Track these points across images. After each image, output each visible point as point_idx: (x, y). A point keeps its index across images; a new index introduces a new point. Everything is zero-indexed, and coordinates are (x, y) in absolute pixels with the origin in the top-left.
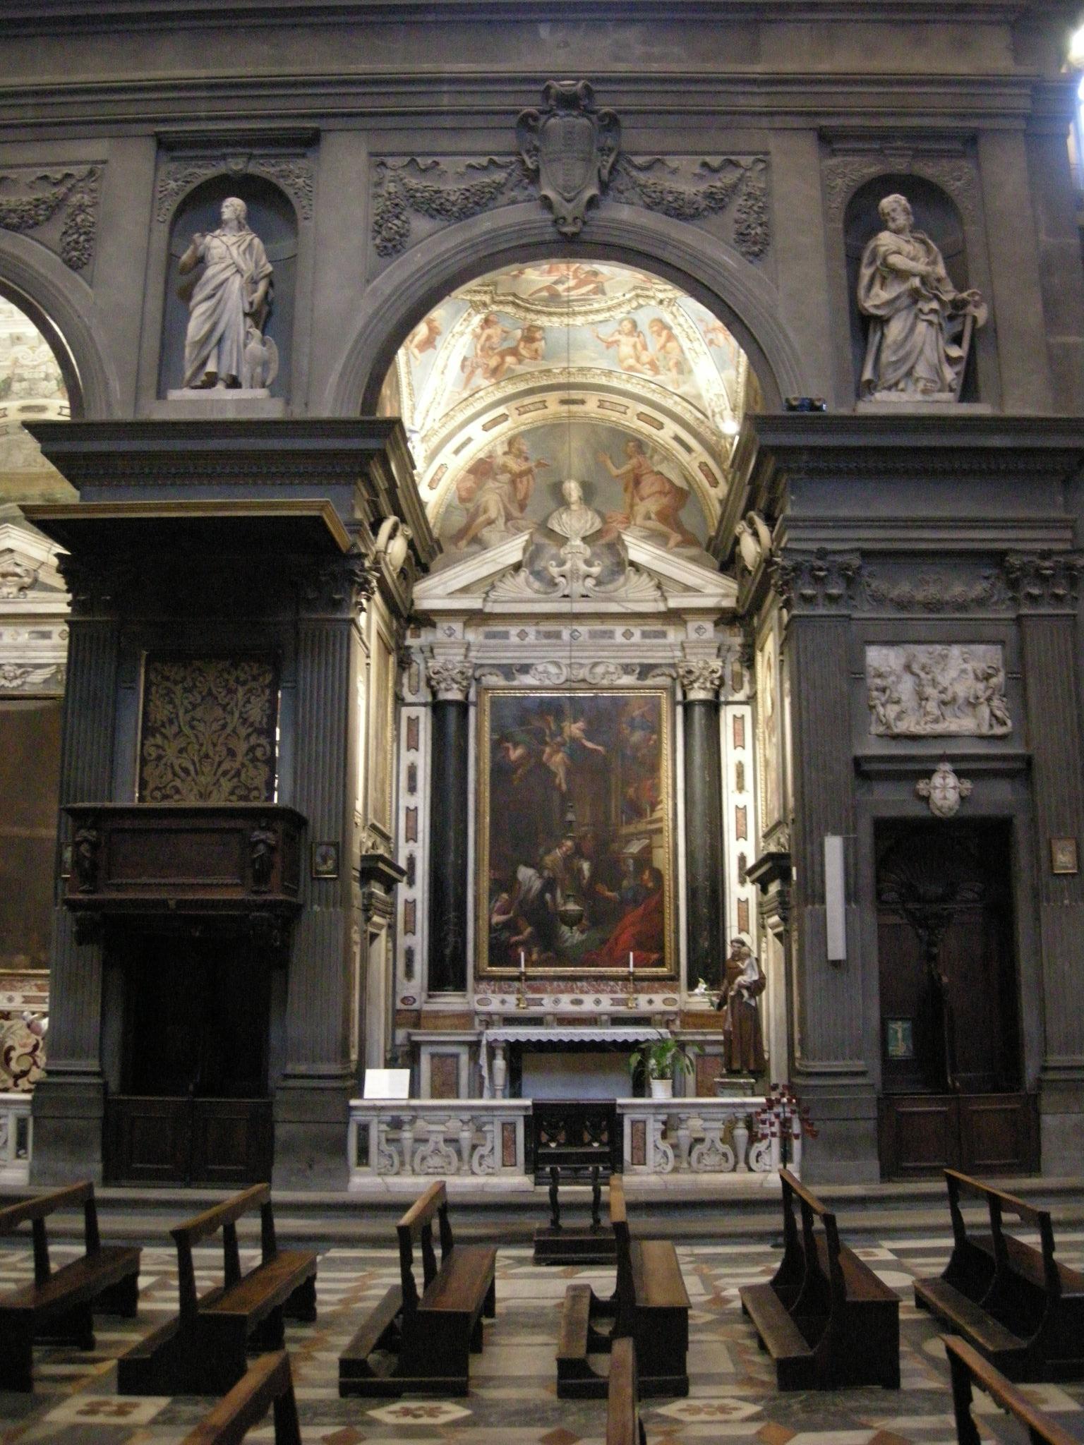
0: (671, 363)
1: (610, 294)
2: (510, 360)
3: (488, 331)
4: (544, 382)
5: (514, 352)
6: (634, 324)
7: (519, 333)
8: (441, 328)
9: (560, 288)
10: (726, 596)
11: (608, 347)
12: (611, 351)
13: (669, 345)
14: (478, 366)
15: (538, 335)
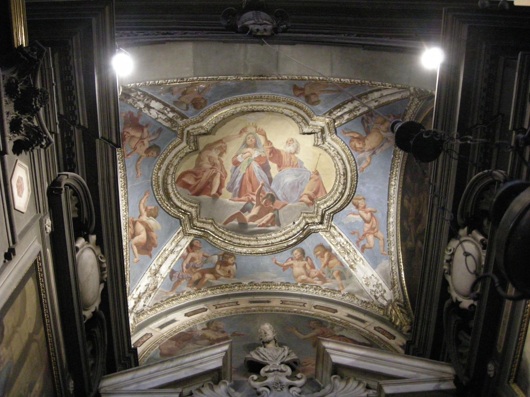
0: (335, 274)
1: (283, 224)
2: (208, 276)
3: (192, 254)
4: (236, 290)
5: (212, 271)
6: (303, 252)
7: (216, 258)
8: (157, 241)
9: (247, 216)
10: (442, 380)
11: (284, 270)
13: (331, 262)
14: (183, 279)
15: (230, 261)
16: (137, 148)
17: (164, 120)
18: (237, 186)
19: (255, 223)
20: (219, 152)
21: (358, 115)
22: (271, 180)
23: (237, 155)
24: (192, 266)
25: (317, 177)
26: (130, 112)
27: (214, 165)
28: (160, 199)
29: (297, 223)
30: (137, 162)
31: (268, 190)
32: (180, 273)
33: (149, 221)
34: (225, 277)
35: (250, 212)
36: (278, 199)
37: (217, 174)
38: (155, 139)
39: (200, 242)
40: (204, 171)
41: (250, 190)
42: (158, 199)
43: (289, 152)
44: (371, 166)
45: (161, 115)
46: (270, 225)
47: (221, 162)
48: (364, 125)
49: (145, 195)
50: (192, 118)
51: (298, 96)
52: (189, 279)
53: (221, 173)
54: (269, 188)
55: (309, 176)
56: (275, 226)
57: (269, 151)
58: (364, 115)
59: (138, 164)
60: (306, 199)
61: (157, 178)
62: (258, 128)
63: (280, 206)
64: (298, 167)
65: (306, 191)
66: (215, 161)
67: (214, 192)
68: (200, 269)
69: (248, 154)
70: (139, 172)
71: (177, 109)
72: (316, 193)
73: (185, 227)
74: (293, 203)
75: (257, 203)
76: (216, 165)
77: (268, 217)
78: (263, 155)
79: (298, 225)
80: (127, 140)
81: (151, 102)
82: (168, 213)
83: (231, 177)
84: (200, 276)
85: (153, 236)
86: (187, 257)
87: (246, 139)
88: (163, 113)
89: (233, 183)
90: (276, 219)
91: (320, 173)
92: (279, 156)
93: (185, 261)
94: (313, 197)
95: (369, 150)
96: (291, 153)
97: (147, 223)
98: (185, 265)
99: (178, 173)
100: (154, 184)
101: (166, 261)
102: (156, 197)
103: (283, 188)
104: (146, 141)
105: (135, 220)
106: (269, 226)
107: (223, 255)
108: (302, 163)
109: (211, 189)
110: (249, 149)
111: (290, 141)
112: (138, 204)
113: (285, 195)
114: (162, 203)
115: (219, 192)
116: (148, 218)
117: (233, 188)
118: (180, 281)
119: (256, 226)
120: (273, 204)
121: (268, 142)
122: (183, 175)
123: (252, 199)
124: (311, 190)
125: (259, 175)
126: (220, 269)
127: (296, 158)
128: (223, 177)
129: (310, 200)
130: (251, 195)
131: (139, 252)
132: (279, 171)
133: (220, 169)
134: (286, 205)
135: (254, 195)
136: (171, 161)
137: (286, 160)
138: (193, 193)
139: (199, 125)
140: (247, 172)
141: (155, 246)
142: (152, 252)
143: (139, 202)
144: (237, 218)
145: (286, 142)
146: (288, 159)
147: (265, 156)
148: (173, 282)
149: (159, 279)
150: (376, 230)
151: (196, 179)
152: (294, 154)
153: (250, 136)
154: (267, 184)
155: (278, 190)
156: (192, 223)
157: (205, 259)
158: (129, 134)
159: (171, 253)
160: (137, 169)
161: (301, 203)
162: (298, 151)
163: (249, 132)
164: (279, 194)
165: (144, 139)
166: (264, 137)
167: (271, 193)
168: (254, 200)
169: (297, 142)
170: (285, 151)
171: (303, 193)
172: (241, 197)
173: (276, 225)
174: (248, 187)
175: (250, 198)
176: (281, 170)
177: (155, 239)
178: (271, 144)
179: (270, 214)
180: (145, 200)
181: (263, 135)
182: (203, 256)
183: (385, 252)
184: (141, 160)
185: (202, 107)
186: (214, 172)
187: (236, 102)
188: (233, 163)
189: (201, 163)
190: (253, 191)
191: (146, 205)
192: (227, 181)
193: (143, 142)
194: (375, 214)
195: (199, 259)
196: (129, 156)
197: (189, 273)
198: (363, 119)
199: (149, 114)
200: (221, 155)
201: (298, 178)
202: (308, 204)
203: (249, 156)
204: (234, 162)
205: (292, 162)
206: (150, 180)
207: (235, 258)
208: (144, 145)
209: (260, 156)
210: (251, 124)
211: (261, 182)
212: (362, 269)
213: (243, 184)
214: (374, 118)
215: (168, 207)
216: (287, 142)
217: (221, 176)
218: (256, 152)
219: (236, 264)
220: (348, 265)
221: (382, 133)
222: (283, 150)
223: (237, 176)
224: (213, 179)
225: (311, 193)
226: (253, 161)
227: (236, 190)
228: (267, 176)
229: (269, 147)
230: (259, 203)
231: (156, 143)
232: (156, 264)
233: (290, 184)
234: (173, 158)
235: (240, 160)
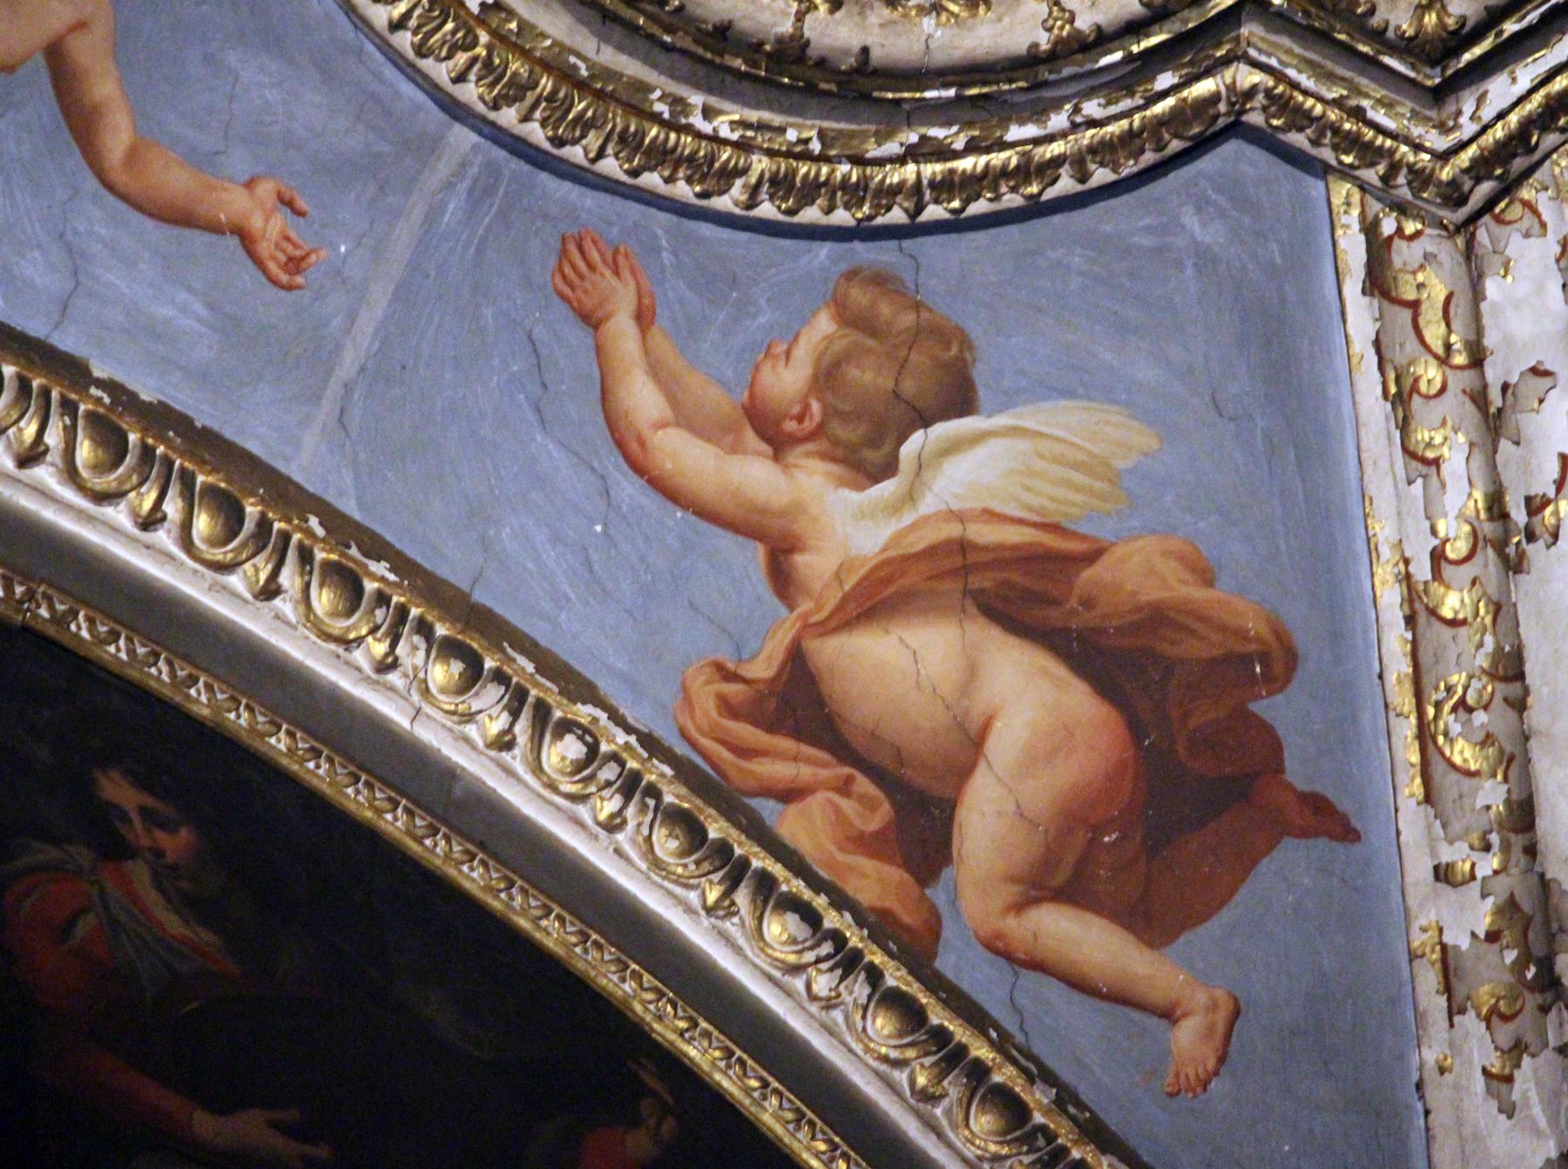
28: (780, 185)
33: (929, 504)
42: (767, 210)
49: (592, 320)
61: (498, 36)
70: (234, 203)
73: (1370, 154)
82: (1036, 210)
85: (1152, 593)
97: (931, 552)
100: (536, 133)
101: (1536, 716)
102: (723, 203)
112: (629, 488)
114: (854, 193)
116: (887, 488)
142: (1298, 771)
143: (612, 462)
156: (1378, 36)
159: (1514, 565)
160: (180, 217)
177: (1198, 594)
180: (656, 371)
184: (104, 87)
191: (718, 399)
206: (463, 137)
215: (966, 164)
232: (1458, 854)
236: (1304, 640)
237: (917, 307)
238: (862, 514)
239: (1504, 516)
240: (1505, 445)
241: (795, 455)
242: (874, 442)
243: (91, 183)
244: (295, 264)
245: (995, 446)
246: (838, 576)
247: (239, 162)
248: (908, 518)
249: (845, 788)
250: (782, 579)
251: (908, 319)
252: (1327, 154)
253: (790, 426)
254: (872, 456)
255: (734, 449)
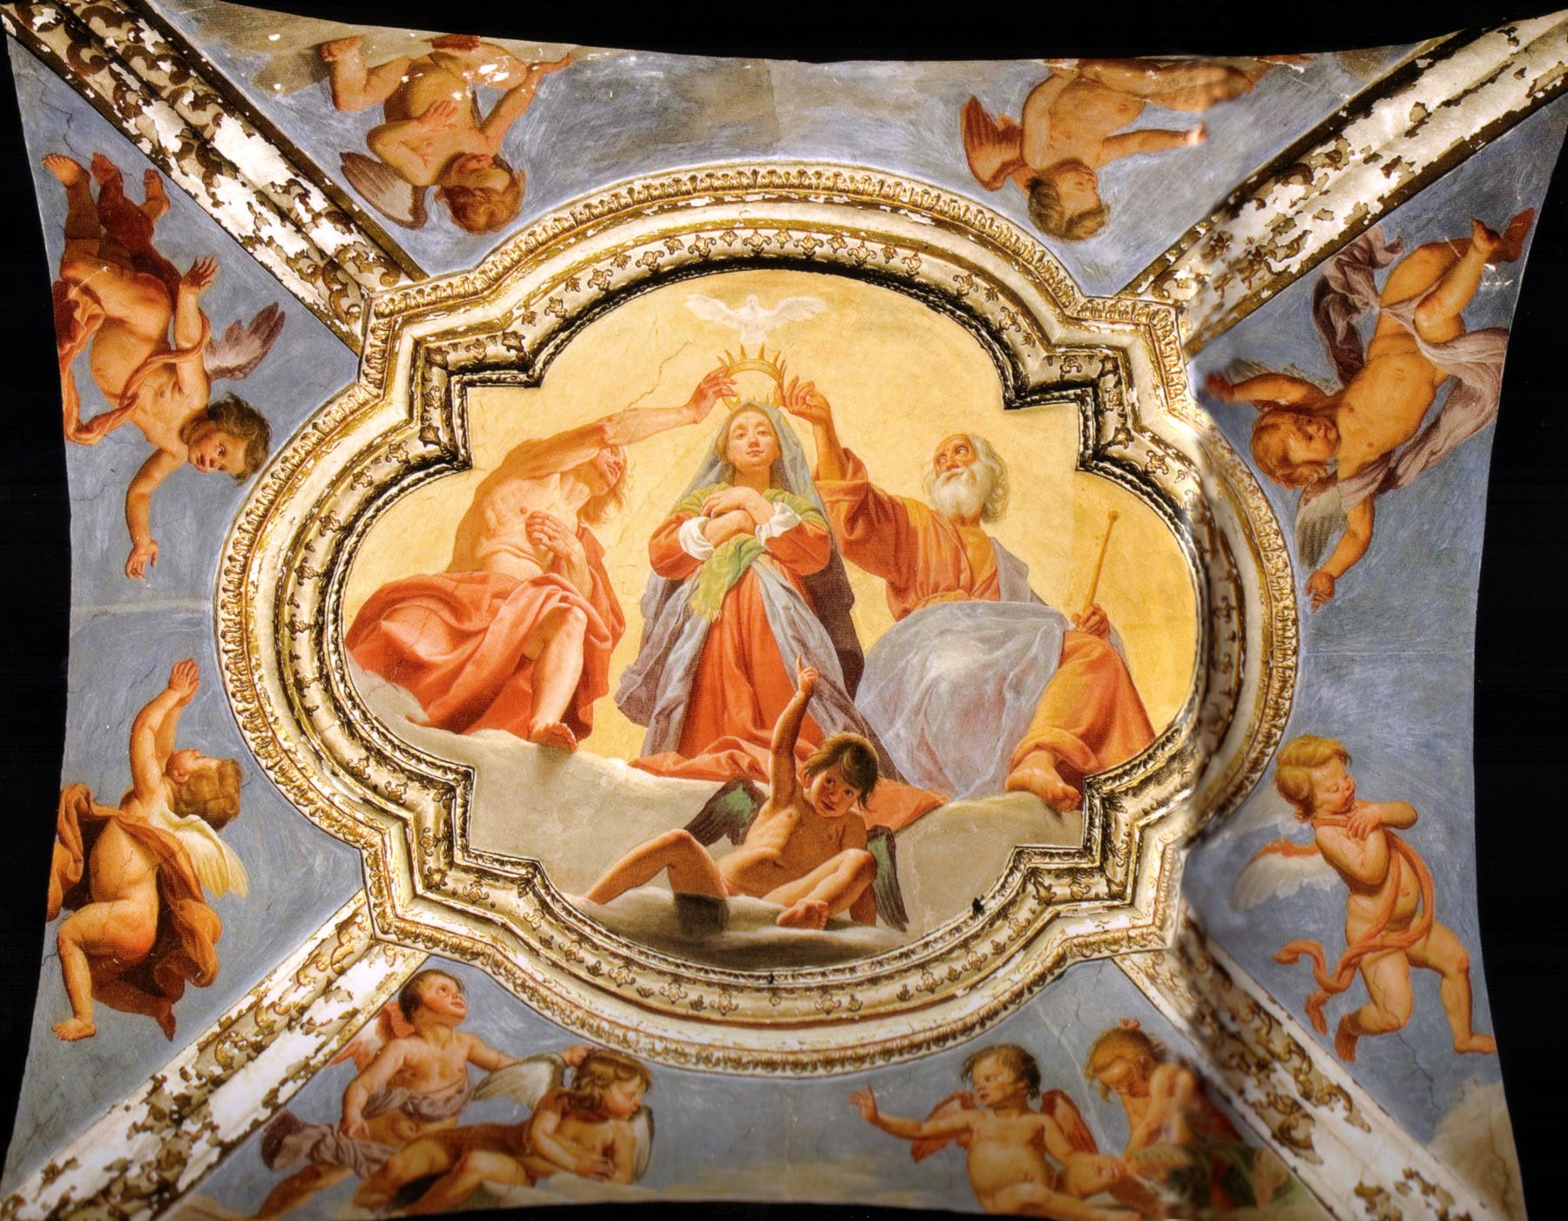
2: (486, 1166)
3: (407, 1048)
7: (540, 1078)
8: (215, 957)
9: (725, 859)
12: (936, 1163)
14: (339, 1163)
15: (620, 1095)
16: (139, 401)
17: (288, 260)
18: (674, 689)
19: (767, 903)
20: (584, 493)
21: (1294, 269)
22: (853, 664)
23: (679, 521)
24: (403, 1108)
25: (1097, 648)
26: (101, 165)
27: (557, 562)
29: (992, 906)
30: (135, 482)
31: (841, 719)
32: (324, 1136)
33: (180, 835)
34: (581, 1173)
35: (738, 839)
36: (891, 773)
37: (571, 617)
38: (240, 368)
39: (460, 987)
40: (502, 595)
41: (742, 715)
43: (948, 511)
44: (1372, 560)
45: (274, 228)
46: (845, 915)
47: (594, 554)
48: (1329, 329)
49: (171, 685)
50: (440, 278)
51: (990, 184)
52: (376, 1168)
53: (593, 611)
54: (846, 709)
55: (1058, 642)
56: (873, 923)
57: (844, 508)
58: (1328, 268)
59: (142, 496)
60: (1041, 772)
62: (787, 381)
63: (903, 815)
64: (998, 591)
65: (1044, 729)
66: (560, 545)
67: (550, 713)
68: (446, 1124)
69: (734, 518)
70: (144, 539)
71: (359, 204)
72: (1095, 739)
74: (972, 797)
75: (777, 790)
76: (564, 564)
77: (836, 869)
78: (816, 524)
79: (1003, 913)
80: (85, 335)
81: (217, 120)
83: (646, 639)
84: (441, 1158)
85: (198, 926)
86: (377, 1057)
87: (727, 438)
88: (284, 215)
89: (652, 676)
90: (878, 884)
91: (1115, 622)
92: (898, 534)
93: (366, 1079)
94: (1078, 760)
95: (1361, 471)
96: (962, 520)
97: (164, 845)
98: (360, 1098)
99: (358, 591)
103: (917, 711)
104: (189, 369)
105: (98, 810)
106: (841, 925)
107: (583, 1067)
108: (1020, 570)
109: (534, 699)
110: (741, 493)
111: (957, 450)
112: (126, 730)
113: (931, 754)
115: (576, 721)
116: (176, 818)
117: (653, 699)
118: (318, 1176)
119: (770, 918)
120: (863, 799)
121: (843, 459)
122: (388, 601)
123: (755, 768)
124: (1066, 727)
125: (790, 633)
126: (559, 1129)
127: (987, 543)
128: (604, 639)
129: (1067, 780)
130: (744, 744)
131: (101, 988)
132: (899, 618)
133: (588, 586)
134: (935, 806)
135: (765, 743)
136: (319, 503)
137: (932, 554)
138: (440, 709)
139: (478, 315)
140: (729, 615)
141: (203, 978)
142: (177, 1008)
143: (132, 719)
144: (671, 866)
145: (931, 455)
146: (947, 555)
147: (824, 530)
148: (277, 1177)
149: (200, 1147)
150: (1416, 923)
151: (459, 637)
152: (975, 521)
153: (750, 418)
154: (833, 685)
155: (891, 722)
157: (479, 1076)
158: (97, 300)
159: (289, 1027)
160: (130, 523)
161: (1017, 795)
162: (998, 506)
163: (744, 400)
164: (897, 741)
165: (182, 352)
166: (819, 430)
167: (855, 736)
168: (765, 780)
169: (992, 455)
170: (932, 507)
171: (1029, 741)
172: (692, 756)
173: (880, 921)
174: (731, 694)
175: (745, 763)
176: (906, 612)
177: (208, 940)
178: (859, 466)
179: (851, 857)
180: (167, 716)
181: (814, 420)
182: (471, 1059)
183: (1476, 1042)
185: (493, 224)
186: (554, 603)
187: (671, 201)
188: (653, 564)
189: (486, 546)
190: (760, 720)
191: (172, 743)
192: (623, 660)
193: (171, 369)
194: (1403, 836)
195: (442, 1075)
196: (94, 438)
197: (376, 1137)
198: (1323, 288)
199: (205, 201)
200: (591, 512)
201: (998, 654)
202: (1054, 805)
203: (740, 530)
204: (662, 558)
205: (964, 564)
207: (647, 1084)
208: (177, 387)
209: (799, 530)
210: (753, 355)
211: (802, 678)
212: (1344, 1145)
213: (707, 681)
214: (1380, 276)
216: (938, 461)
217: (591, 629)
218: (778, 507)
219: (650, 1114)
220: (1266, 1132)
221: (1428, 352)
222: (917, 504)
223: (676, 635)
224: (546, 644)
225: (1069, 740)
226: (764, 559)
227: (667, 713)
228: (835, 642)
229: (848, 483)
230: (788, 794)
231: (251, 393)
233: (956, 689)
234: (333, 484)
235: (694, 550)
236: (217, 981)
237: (238, 791)
238: (163, 814)
239: (302, 1014)
240: (322, 1000)
241: (168, 780)
242: (188, 804)
243: (126, 488)
244: (135, 572)
245: (210, 844)
246: (139, 819)
247: (158, 534)
248: (171, 830)
249: (76, 861)
250: (128, 800)
251: (232, 791)
252: (369, 883)
253: (176, 773)
254: (183, 807)
255: (158, 758)
